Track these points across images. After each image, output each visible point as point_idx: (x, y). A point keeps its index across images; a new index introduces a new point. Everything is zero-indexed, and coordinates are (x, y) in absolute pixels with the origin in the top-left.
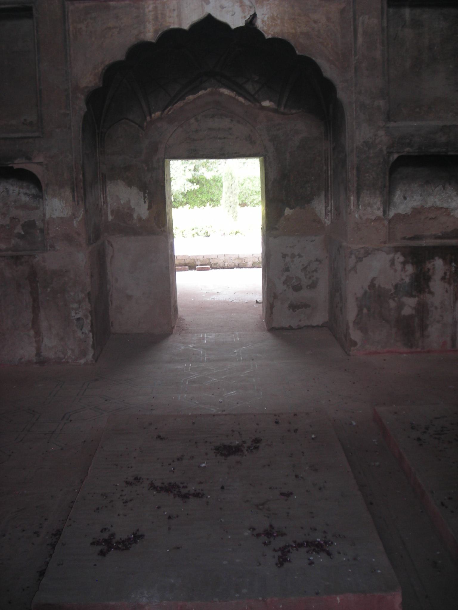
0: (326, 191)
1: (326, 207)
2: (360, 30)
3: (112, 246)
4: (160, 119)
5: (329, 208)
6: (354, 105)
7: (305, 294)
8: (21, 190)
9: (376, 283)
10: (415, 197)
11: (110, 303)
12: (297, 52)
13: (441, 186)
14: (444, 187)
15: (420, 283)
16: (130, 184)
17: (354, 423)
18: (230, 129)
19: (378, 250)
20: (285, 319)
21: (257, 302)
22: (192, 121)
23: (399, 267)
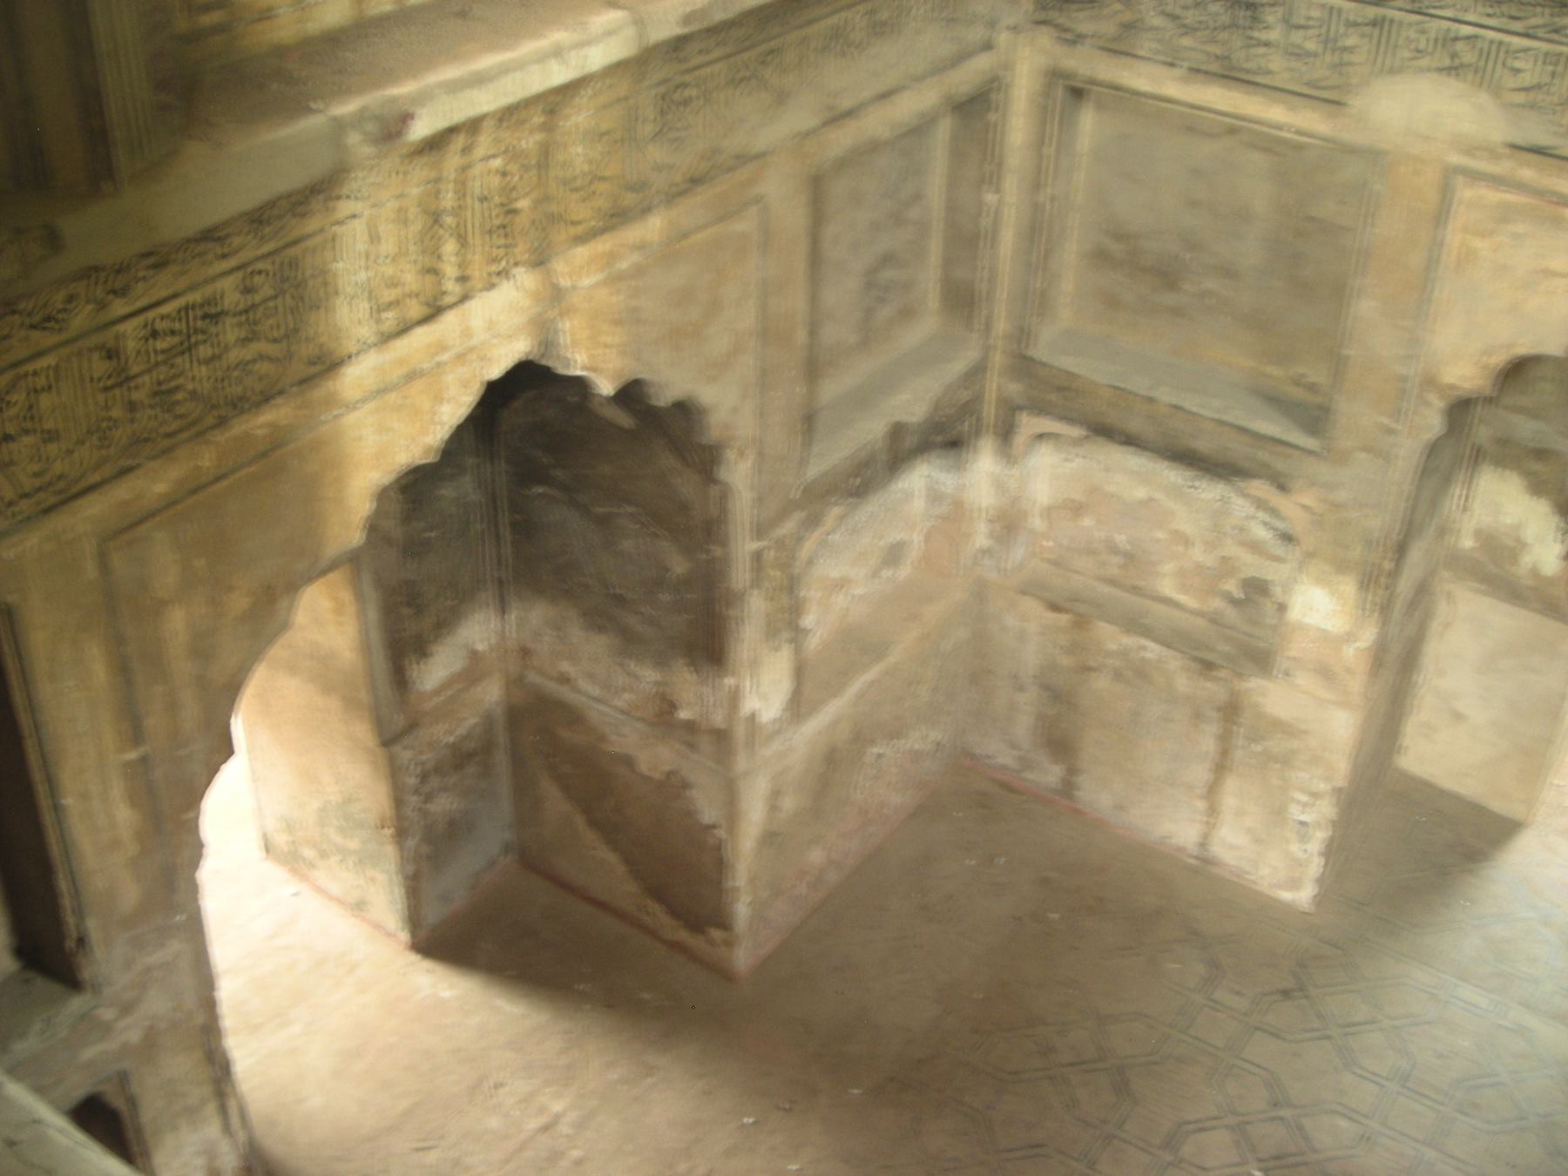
16: (1537, 487)
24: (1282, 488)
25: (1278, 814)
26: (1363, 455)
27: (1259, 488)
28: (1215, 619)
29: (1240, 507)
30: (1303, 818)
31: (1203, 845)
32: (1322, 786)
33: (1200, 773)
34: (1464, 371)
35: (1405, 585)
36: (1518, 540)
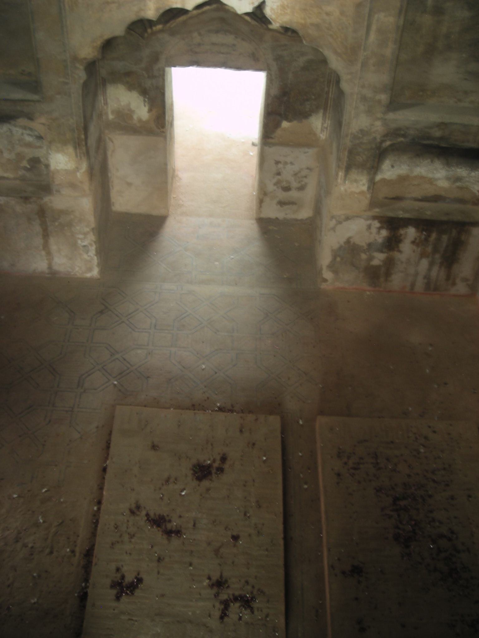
0: (325, 109)
1: (323, 124)
2: (374, 27)
3: (112, 142)
4: (161, 31)
5: (325, 125)
6: (355, 96)
7: (294, 194)
8: (24, 131)
9: (352, 241)
10: (403, 167)
11: (111, 187)
12: (304, 42)
13: (429, 160)
14: (432, 161)
15: (392, 243)
16: (130, 87)
17: (301, 422)
18: (234, 45)
19: (357, 217)
20: (272, 211)
21: (253, 144)
22: (195, 34)
23: (374, 230)
24: (30, 117)
25: (74, 246)
26: (58, 97)
27: (22, 121)
28: (23, 179)
29: (17, 131)
30: (85, 243)
31: (50, 267)
32: (87, 229)
33: (38, 241)
34: (88, 52)
35: (92, 141)
36: (130, 110)
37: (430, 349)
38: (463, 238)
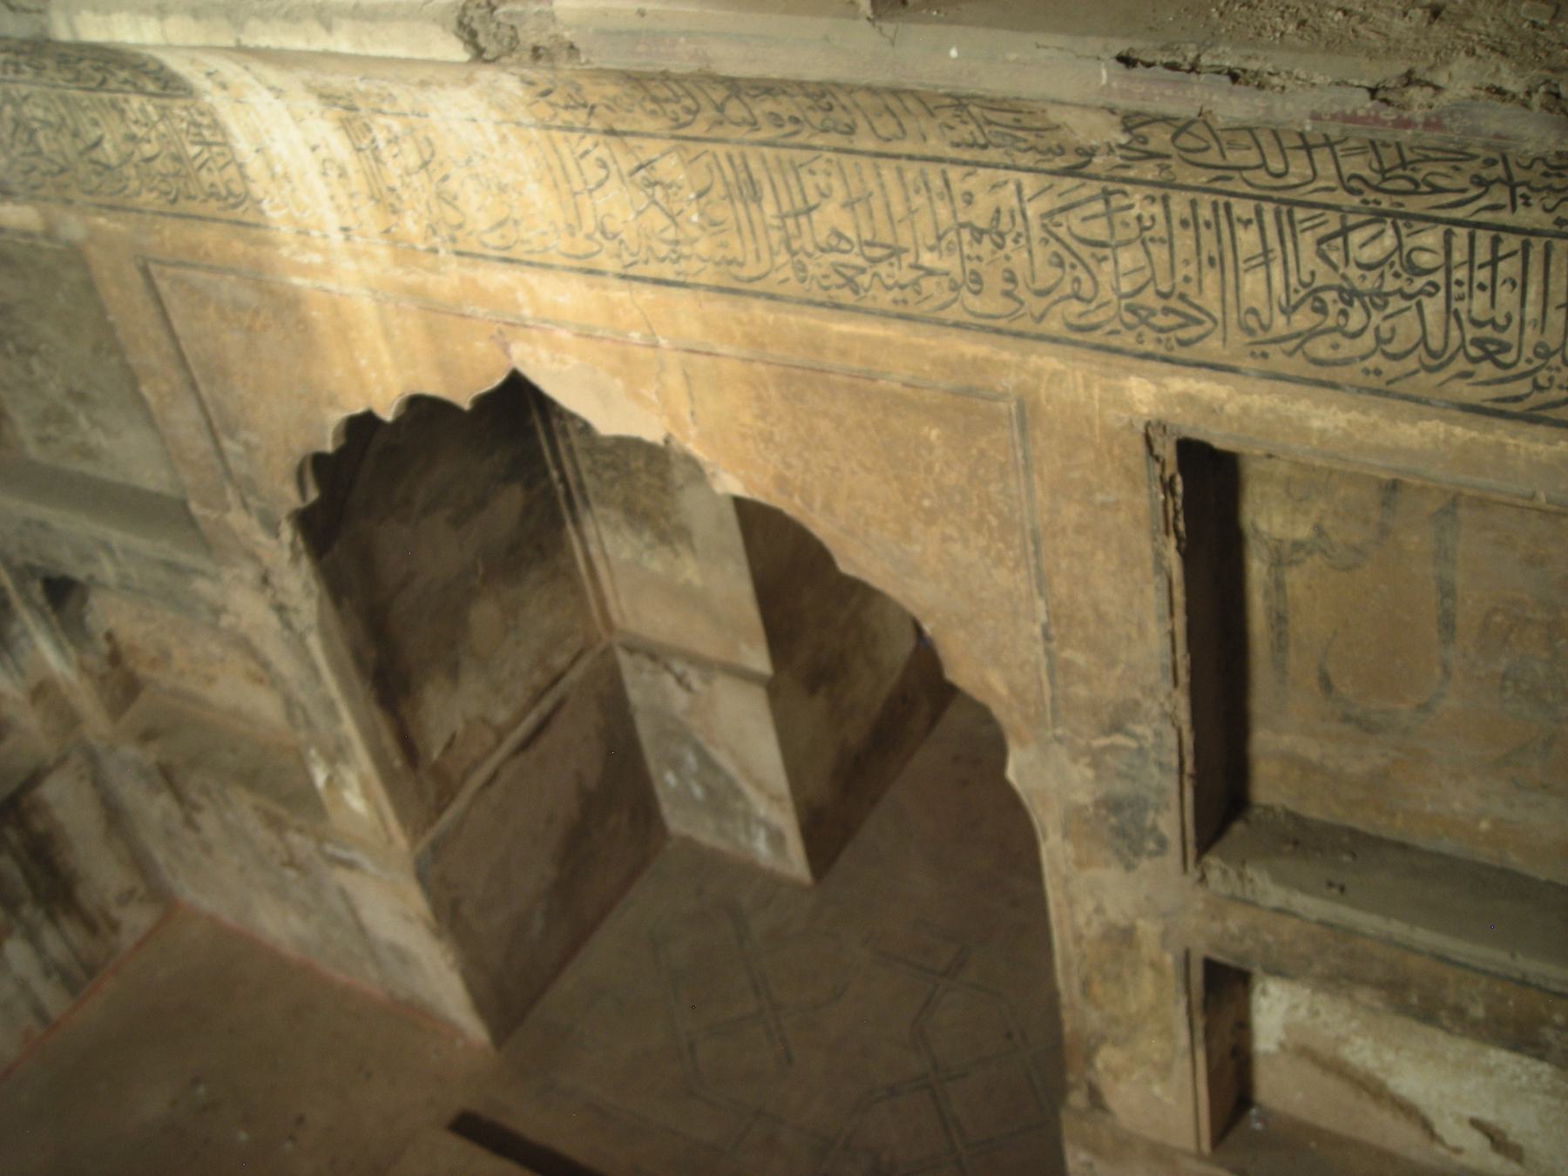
37: (202, 1090)
38: (39, 826)
